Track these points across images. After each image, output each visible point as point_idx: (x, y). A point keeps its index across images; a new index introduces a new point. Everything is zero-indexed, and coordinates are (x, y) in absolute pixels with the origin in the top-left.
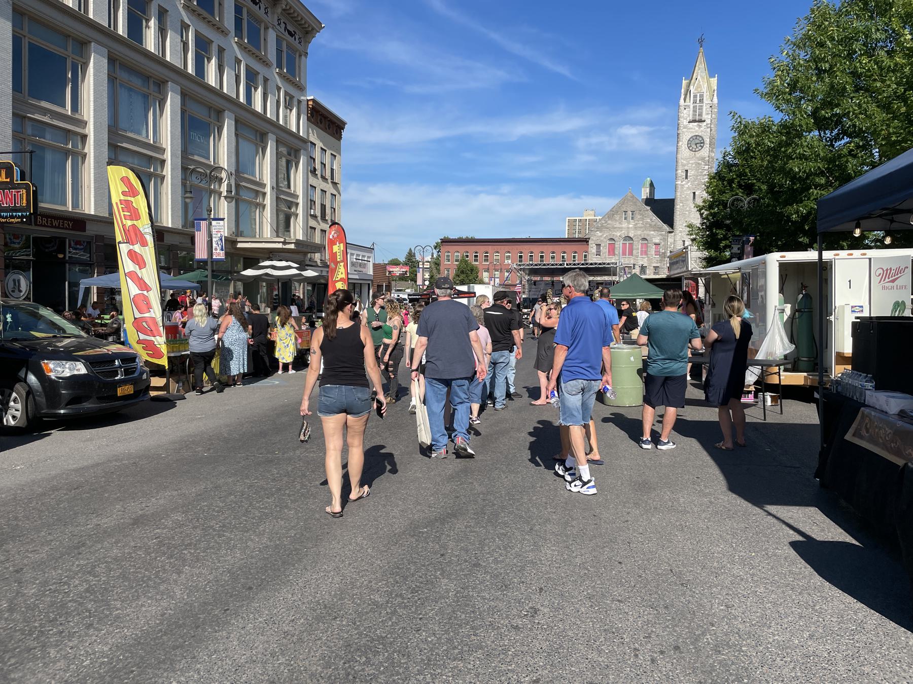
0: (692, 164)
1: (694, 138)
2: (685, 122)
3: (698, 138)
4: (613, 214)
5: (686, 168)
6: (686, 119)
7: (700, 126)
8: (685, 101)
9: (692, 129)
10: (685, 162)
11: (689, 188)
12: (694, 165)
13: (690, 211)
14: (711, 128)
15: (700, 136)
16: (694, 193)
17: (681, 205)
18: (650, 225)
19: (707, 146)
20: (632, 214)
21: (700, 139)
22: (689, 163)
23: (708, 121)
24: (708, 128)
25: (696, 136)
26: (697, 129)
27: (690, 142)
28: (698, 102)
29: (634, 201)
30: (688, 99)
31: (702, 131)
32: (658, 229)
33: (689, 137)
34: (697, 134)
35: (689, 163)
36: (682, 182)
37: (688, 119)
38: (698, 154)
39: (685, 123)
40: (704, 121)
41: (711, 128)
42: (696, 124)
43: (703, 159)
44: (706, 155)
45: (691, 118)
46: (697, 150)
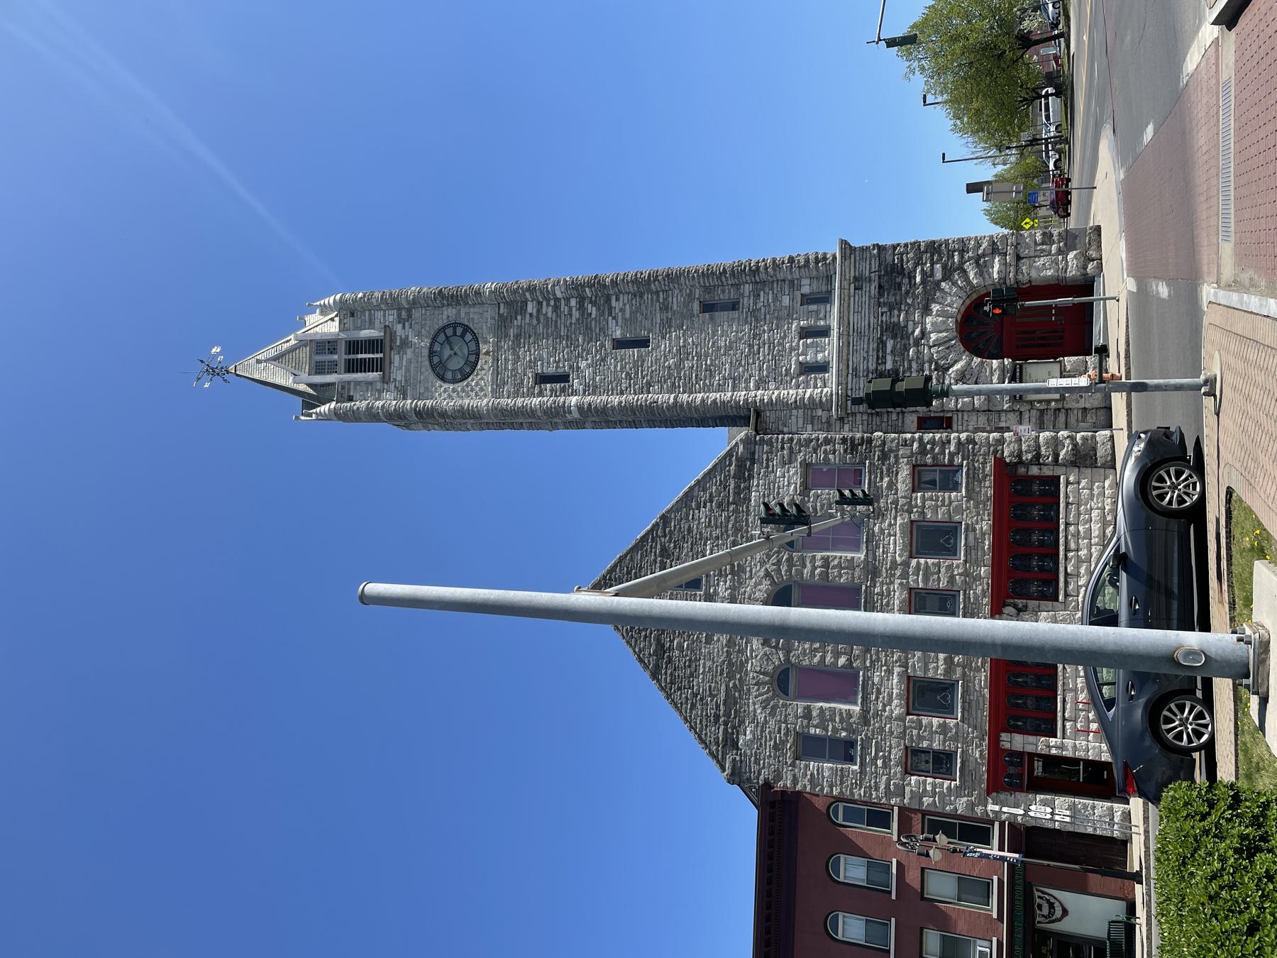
1: (436, 360)
5: (529, 380)
7: (405, 343)
9: (408, 370)
16: (620, 344)
21: (442, 338)
24: (410, 316)
26: (409, 352)
34: (426, 352)
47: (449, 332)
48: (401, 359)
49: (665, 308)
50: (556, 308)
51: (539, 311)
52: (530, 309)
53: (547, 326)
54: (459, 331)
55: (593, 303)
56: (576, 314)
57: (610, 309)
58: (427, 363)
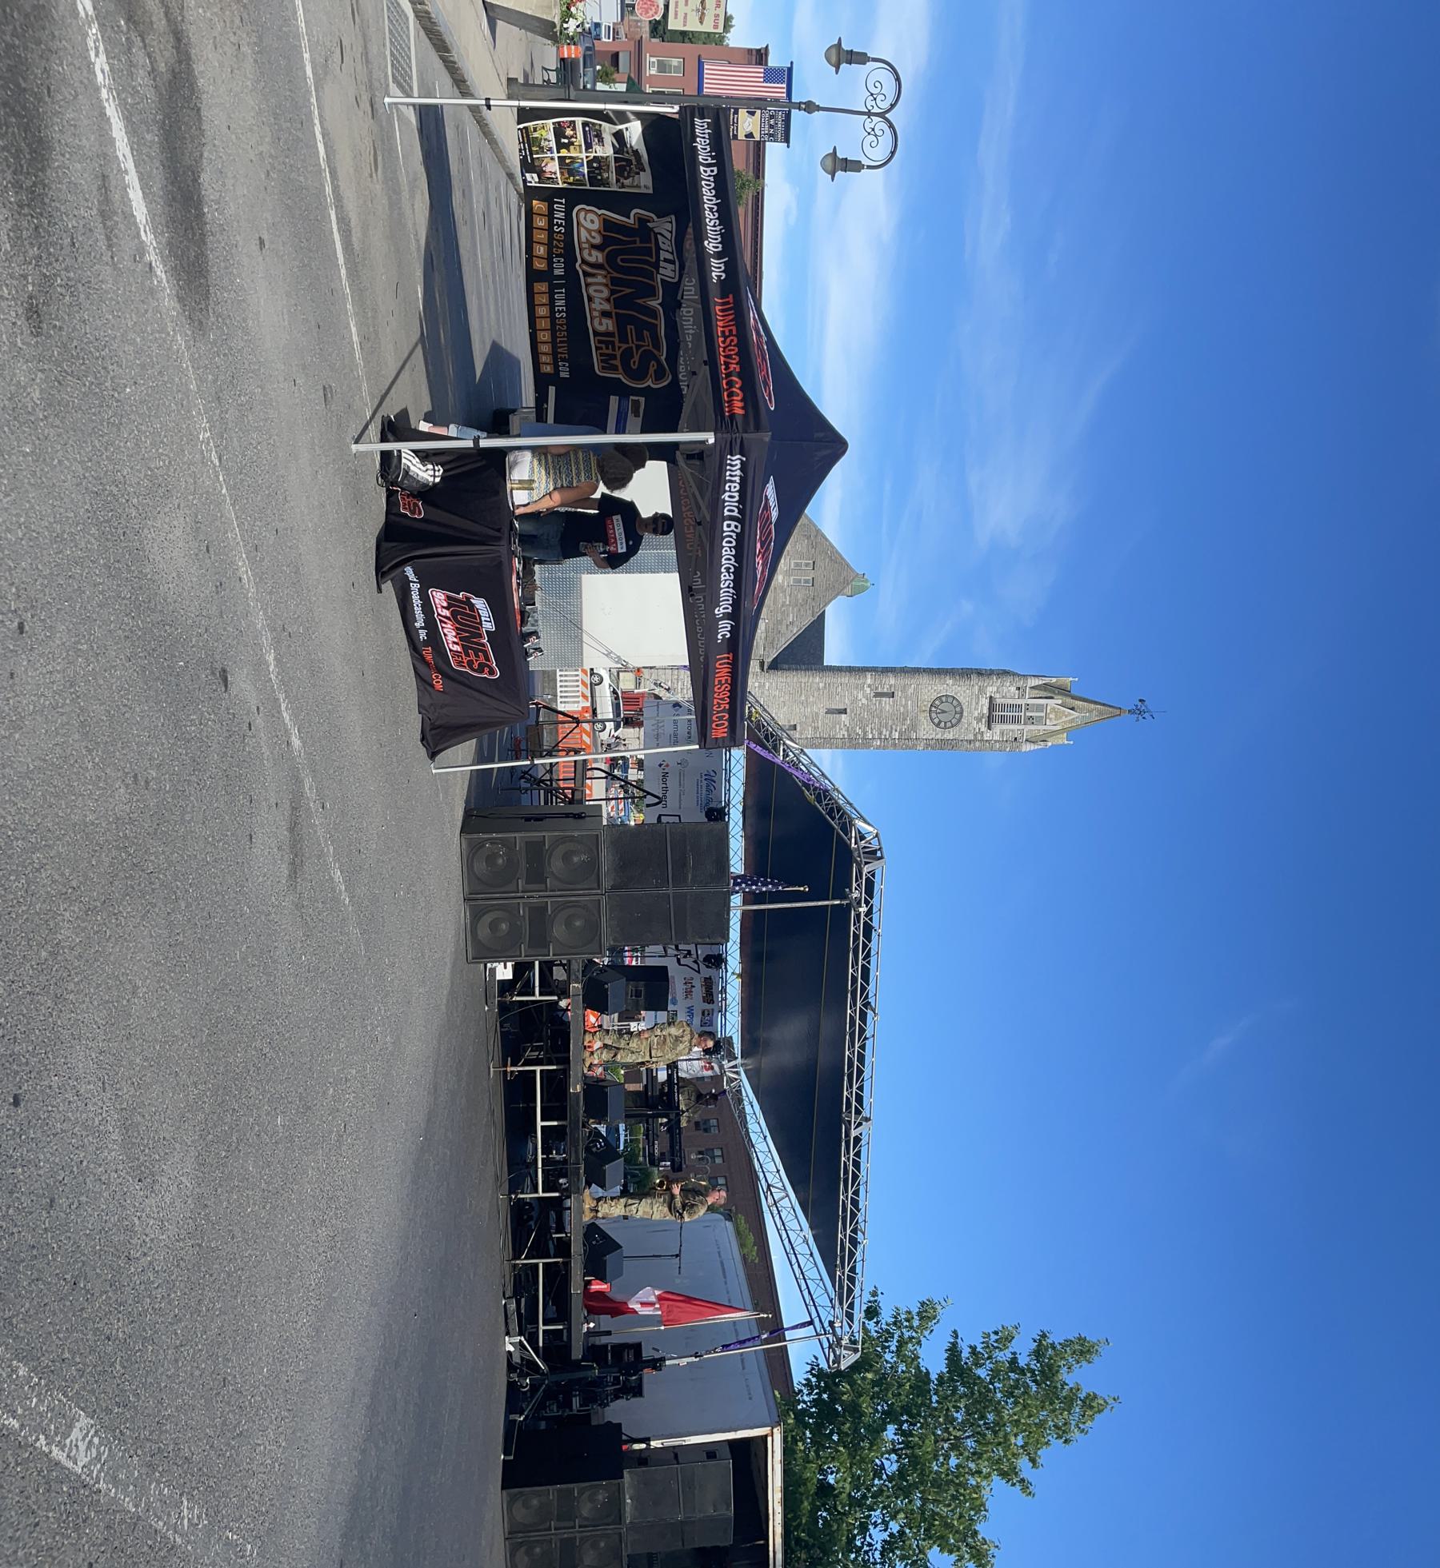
0: (906, 706)
1: (958, 709)
2: (991, 690)
3: (958, 716)
4: (809, 538)
5: (898, 694)
6: (998, 692)
7: (979, 720)
8: (1031, 688)
9: (977, 704)
10: (911, 690)
11: (855, 700)
12: (902, 710)
13: (806, 704)
14: (975, 740)
15: (959, 721)
16: (844, 711)
17: (821, 685)
18: (780, 622)
19: (939, 734)
20: (806, 581)
21: (954, 721)
22: (906, 701)
23: (987, 736)
24: (975, 735)
25: (961, 713)
26: (976, 715)
27: (950, 700)
28: (1029, 714)
29: (837, 586)
30: (1035, 693)
31: (969, 725)
32: (770, 639)
33: (961, 699)
34: (965, 714)
35: (906, 701)
36: (869, 686)
37: (997, 696)
38: (924, 719)
39: (990, 689)
40: (989, 728)
41: (975, 740)
42: (986, 711)
43: (914, 727)
44: (922, 734)
45: (998, 701)
46: (934, 715)
47: (949, 724)
48: (982, 710)
49: (816, 728)
50: (881, 733)
51: (891, 732)
52: (897, 734)
53: (887, 724)
54: (942, 725)
55: (858, 734)
56: (868, 729)
57: (848, 731)
58: (964, 707)
